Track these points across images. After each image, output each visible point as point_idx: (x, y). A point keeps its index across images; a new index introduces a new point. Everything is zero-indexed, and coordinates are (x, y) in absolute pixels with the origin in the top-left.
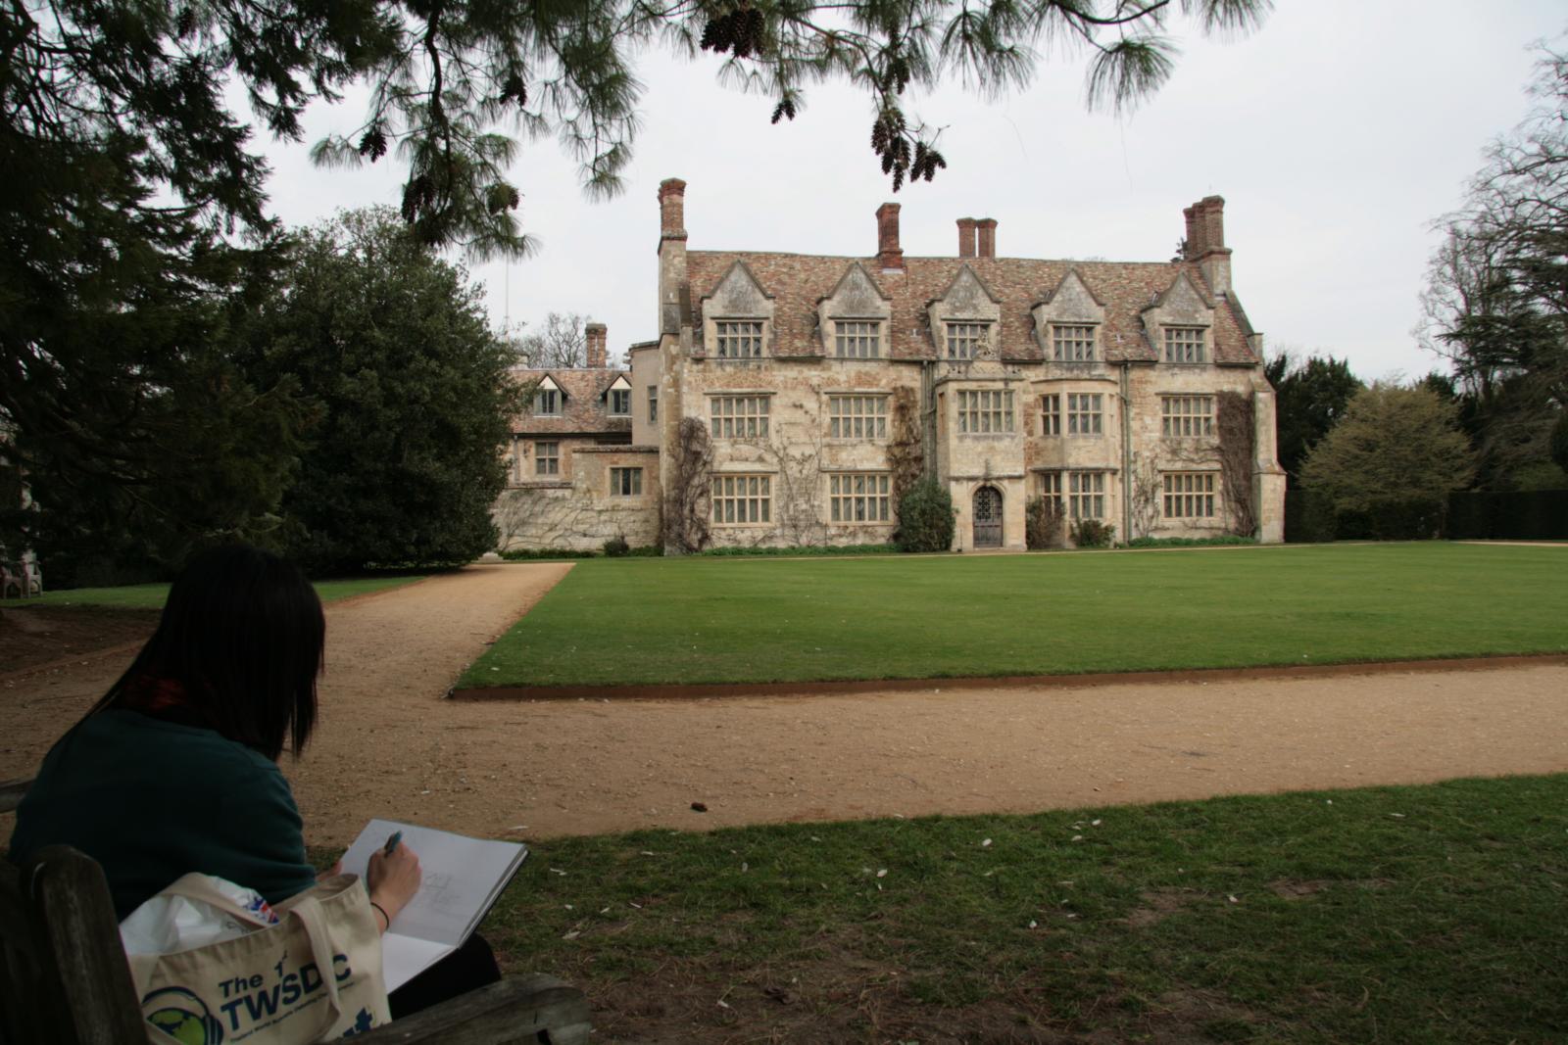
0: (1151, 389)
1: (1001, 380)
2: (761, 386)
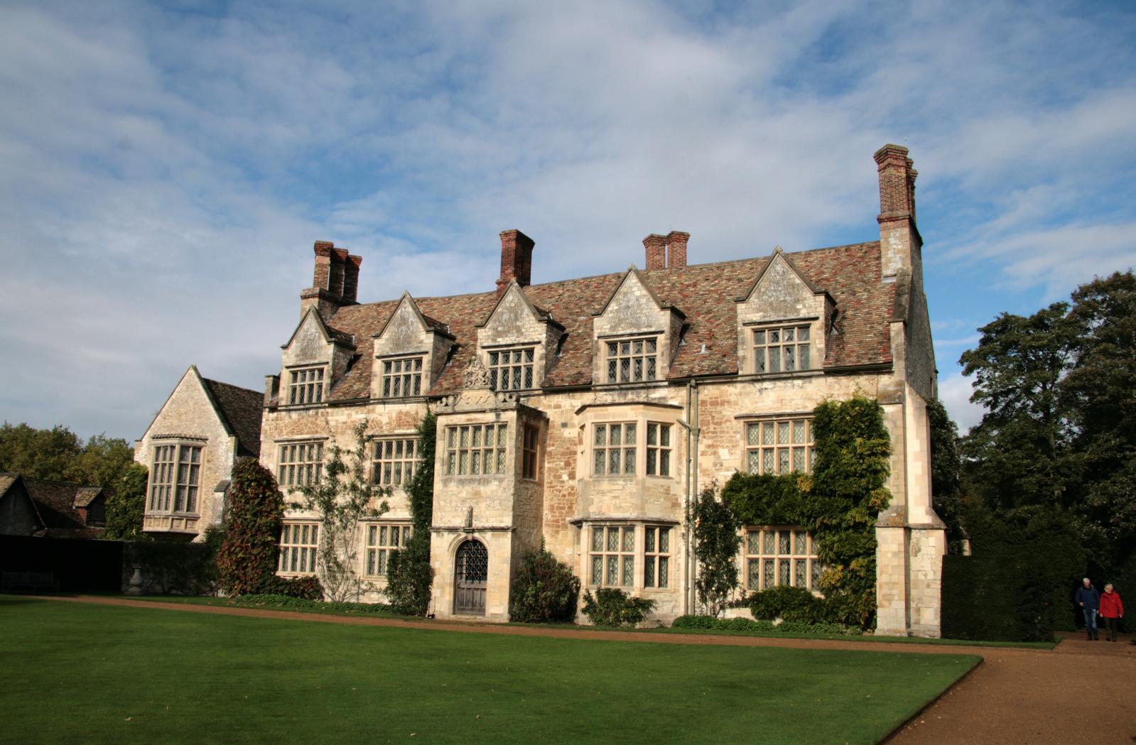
0: (729, 412)
1: (491, 410)
2: (317, 432)
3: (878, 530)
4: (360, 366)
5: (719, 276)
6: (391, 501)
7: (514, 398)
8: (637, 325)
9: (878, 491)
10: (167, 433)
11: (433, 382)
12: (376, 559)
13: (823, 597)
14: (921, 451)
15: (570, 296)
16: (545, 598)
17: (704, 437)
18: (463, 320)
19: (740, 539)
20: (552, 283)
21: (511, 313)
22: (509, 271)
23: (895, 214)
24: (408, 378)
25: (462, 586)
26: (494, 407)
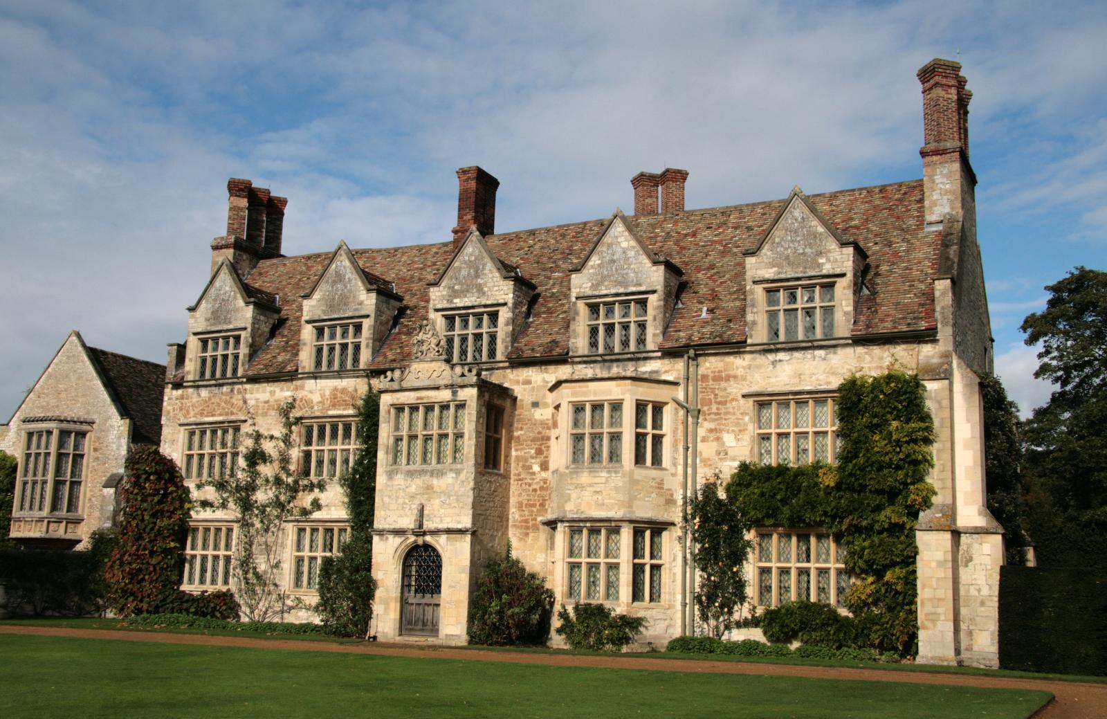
0: (736, 389)
1: (446, 387)
2: (232, 413)
3: (919, 534)
4: (286, 332)
5: (725, 223)
6: (324, 497)
7: (474, 372)
8: (624, 284)
9: (919, 486)
10: (43, 415)
11: (376, 352)
12: (305, 569)
13: (851, 615)
14: (973, 437)
15: (542, 248)
16: (512, 616)
17: (706, 420)
18: (412, 277)
19: (748, 544)
20: (521, 232)
21: (470, 268)
22: (469, 217)
23: (942, 145)
24: (344, 347)
25: (411, 601)
26: (450, 382)
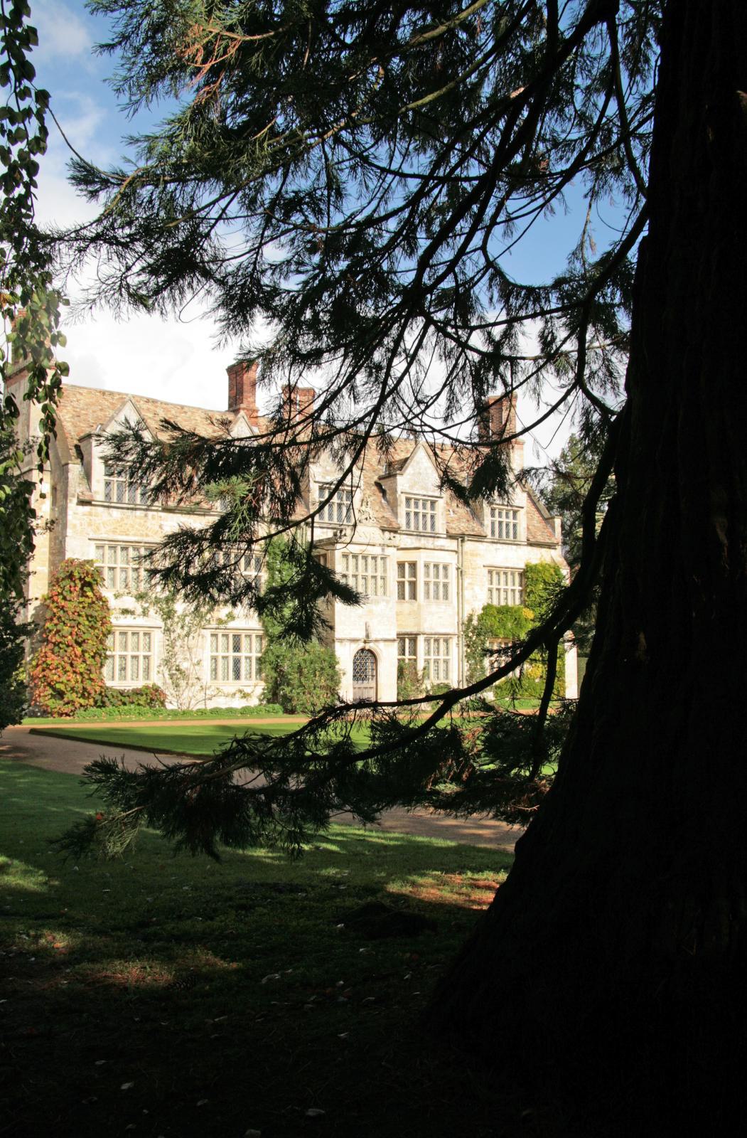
2: (147, 535)
